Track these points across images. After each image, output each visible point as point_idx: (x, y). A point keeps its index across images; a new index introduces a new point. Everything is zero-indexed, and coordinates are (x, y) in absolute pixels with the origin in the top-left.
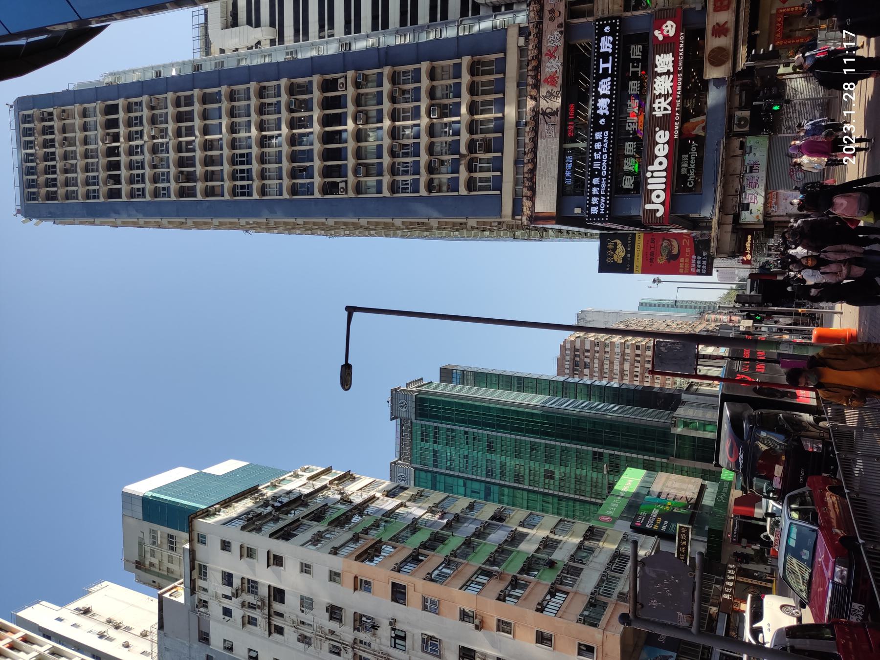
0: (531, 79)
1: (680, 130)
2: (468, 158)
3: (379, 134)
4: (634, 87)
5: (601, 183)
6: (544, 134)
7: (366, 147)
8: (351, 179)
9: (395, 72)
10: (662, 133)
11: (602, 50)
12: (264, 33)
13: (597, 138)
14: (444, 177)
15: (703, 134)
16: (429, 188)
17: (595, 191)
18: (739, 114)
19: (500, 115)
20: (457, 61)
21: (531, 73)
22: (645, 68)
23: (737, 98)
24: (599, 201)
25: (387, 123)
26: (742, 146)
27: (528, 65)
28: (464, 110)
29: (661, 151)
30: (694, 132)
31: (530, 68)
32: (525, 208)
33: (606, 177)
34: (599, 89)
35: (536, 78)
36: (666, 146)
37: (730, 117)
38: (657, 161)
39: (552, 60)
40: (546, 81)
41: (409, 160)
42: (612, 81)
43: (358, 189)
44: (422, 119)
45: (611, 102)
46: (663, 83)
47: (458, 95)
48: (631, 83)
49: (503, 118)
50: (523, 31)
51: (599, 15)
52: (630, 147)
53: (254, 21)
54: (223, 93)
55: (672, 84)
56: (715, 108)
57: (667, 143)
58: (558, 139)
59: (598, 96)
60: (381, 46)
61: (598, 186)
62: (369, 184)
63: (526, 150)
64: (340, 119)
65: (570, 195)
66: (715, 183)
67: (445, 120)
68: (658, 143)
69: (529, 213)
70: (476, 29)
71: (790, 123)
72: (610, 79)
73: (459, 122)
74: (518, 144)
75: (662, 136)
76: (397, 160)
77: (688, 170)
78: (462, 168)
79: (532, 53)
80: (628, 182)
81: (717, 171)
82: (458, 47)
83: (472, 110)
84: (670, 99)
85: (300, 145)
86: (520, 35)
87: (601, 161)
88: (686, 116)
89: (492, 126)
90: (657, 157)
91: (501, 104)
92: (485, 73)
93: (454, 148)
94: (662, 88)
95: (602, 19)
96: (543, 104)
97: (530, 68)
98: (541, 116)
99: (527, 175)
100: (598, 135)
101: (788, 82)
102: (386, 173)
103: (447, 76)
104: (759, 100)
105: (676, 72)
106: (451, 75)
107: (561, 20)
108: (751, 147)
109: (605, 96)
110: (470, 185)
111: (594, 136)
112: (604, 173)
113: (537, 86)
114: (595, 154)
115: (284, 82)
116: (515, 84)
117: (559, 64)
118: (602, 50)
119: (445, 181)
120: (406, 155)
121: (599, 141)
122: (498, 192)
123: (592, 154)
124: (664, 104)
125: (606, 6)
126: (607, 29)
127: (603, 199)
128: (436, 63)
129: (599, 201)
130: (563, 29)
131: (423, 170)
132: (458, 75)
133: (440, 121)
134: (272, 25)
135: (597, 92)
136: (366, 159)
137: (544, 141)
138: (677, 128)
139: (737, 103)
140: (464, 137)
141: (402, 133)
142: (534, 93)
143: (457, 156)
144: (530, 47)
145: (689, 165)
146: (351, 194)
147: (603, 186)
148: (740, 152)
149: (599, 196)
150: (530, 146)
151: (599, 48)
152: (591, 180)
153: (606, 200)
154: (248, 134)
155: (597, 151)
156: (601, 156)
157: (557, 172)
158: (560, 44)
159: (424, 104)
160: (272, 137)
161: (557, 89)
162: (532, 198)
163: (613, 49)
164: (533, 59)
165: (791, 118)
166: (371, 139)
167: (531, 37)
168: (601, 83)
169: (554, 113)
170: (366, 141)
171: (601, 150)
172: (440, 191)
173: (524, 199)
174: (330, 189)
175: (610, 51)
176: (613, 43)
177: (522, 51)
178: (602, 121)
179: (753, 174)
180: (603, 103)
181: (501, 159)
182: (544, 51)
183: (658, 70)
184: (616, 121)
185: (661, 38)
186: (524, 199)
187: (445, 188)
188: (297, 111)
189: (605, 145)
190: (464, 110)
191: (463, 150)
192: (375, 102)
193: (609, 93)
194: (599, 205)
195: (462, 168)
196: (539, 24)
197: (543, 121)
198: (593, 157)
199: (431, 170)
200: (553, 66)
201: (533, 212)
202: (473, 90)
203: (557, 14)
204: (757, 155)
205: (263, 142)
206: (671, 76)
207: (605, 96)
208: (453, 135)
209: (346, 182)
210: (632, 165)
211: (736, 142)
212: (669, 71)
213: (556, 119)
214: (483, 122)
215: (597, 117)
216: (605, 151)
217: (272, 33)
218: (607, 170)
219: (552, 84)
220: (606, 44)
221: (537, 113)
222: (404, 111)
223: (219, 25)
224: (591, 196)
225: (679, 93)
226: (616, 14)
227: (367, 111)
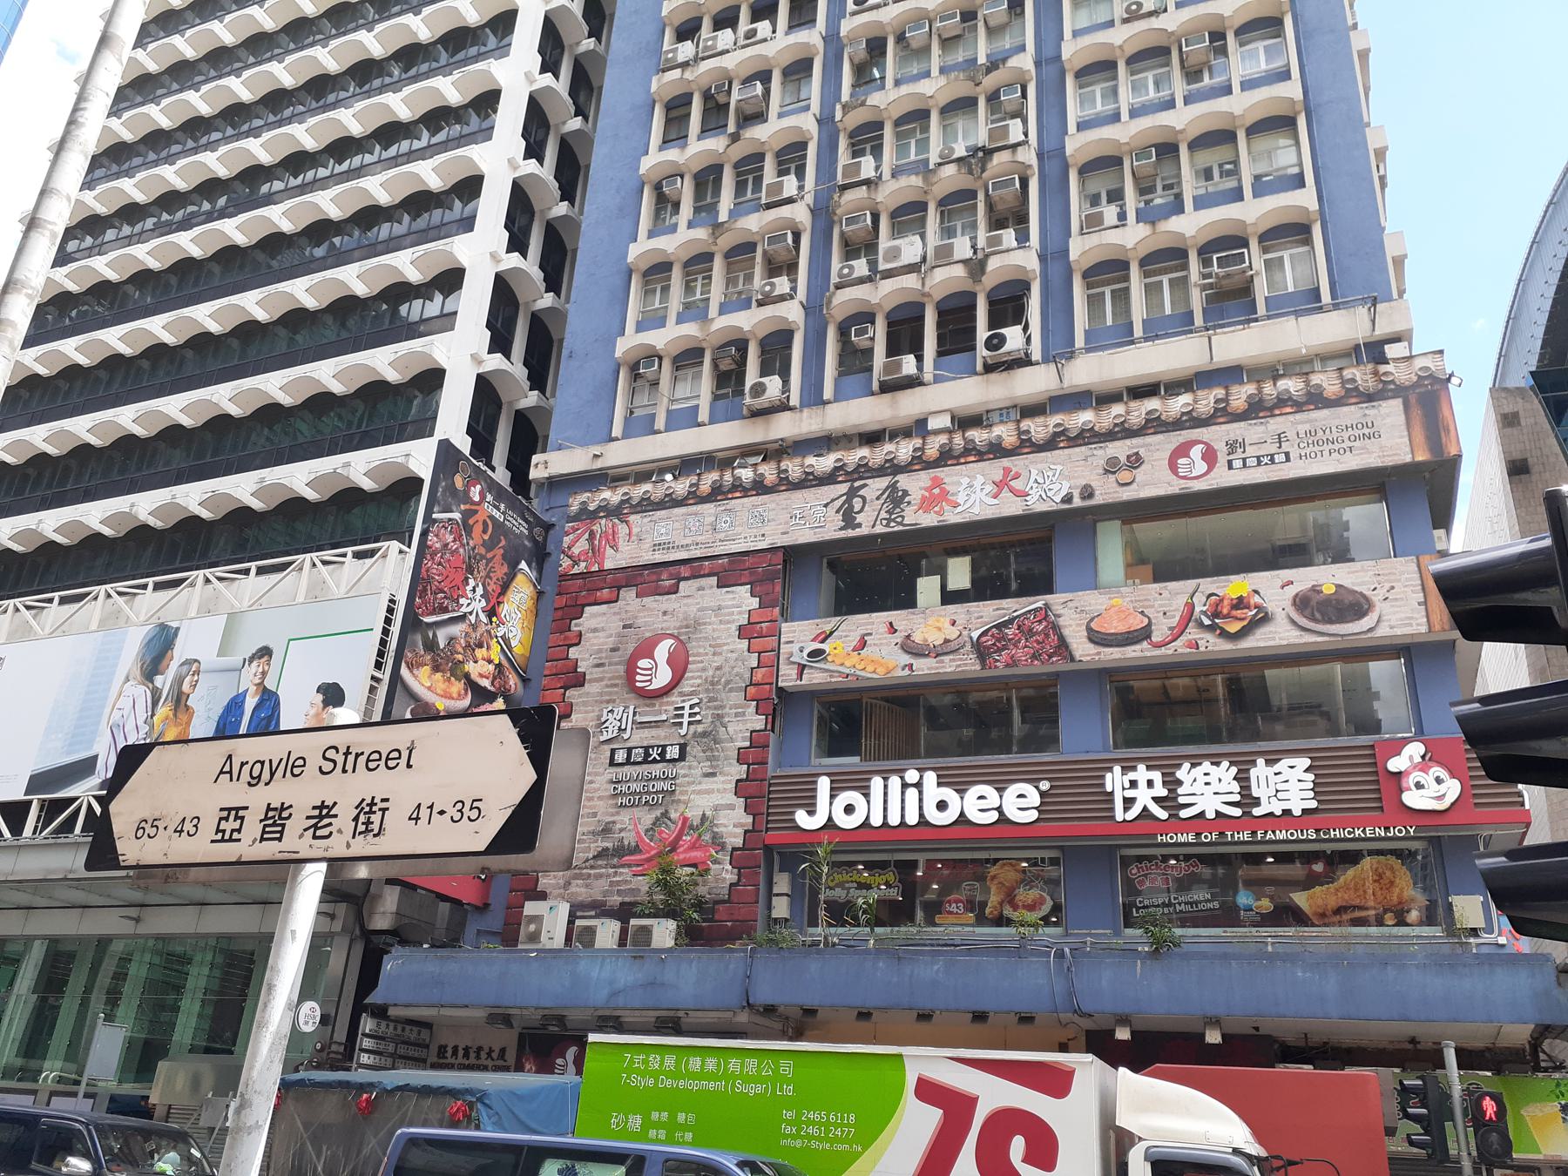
55: (1210, 815)
84: (1162, 814)
94: (1199, 787)
183: (1260, 771)
206: (1237, 812)
212: (1257, 802)
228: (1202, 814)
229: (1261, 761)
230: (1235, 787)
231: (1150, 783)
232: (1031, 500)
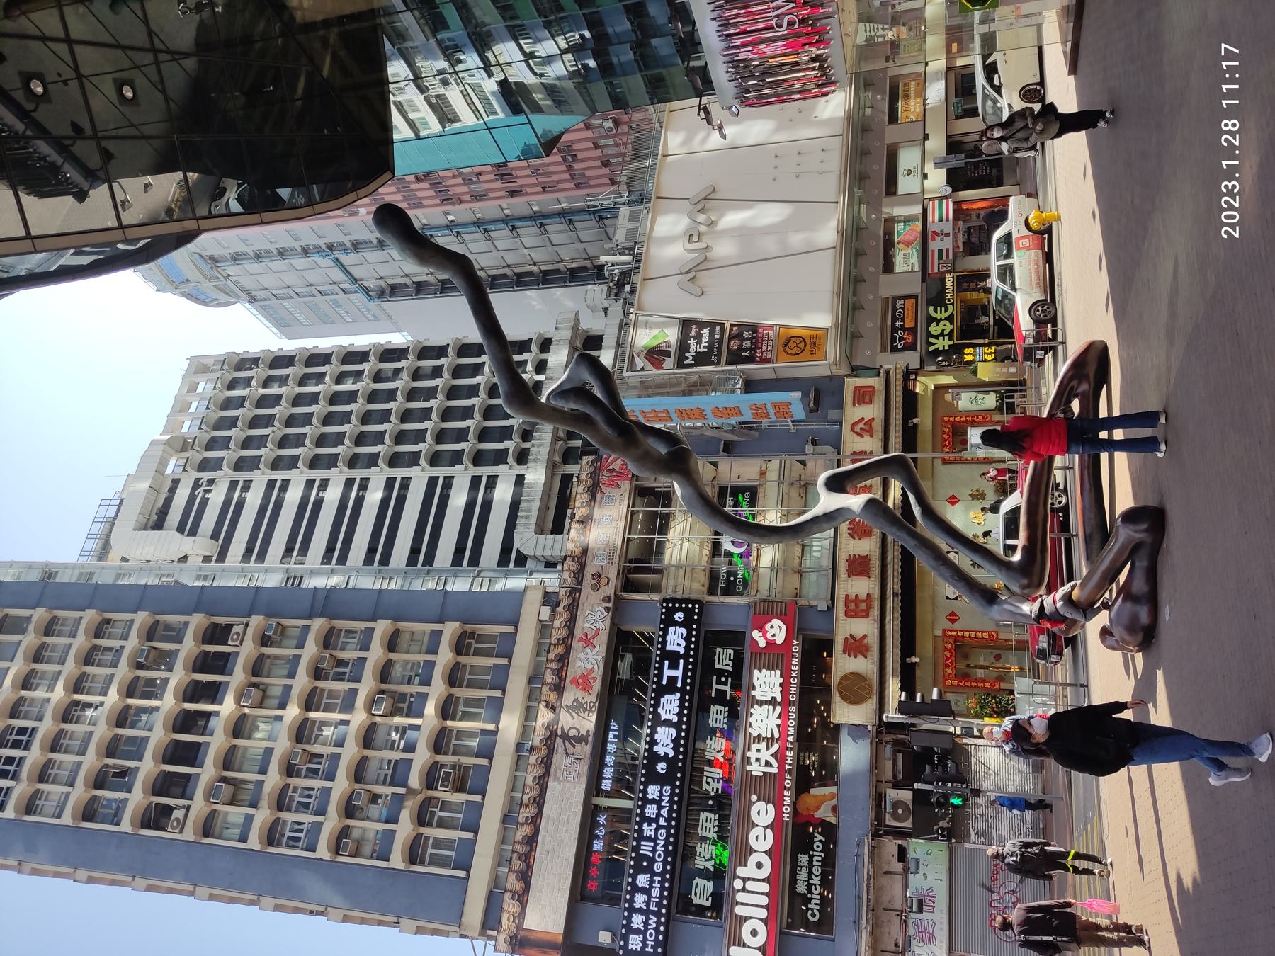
0: (552, 676)
1: (794, 805)
2: (421, 797)
3: (274, 734)
4: (718, 716)
5: (651, 887)
6: (560, 774)
7: (246, 748)
8: (199, 805)
9: (332, 628)
10: (761, 805)
11: (668, 648)
12: (199, 546)
13: (650, 796)
14: (367, 828)
15: (833, 820)
16: (337, 848)
17: (640, 900)
18: (893, 794)
19: (491, 727)
20: (370, 624)
21: (553, 665)
22: (737, 686)
23: (889, 764)
24: (646, 924)
25: (293, 712)
26: (902, 854)
27: (548, 652)
28: (430, 709)
29: (761, 840)
30: (818, 815)
31: (551, 656)
32: (505, 917)
33: (662, 874)
34: (660, 710)
35: (560, 673)
36: (769, 832)
37: (879, 798)
38: (752, 860)
39: (588, 650)
40: (574, 681)
41: (316, 784)
42: (682, 700)
43: (207, 829)
44: (355, 712)
45: (678, 736)
46: (764, 717)
47: (427, 682)
48: (714, 708)
49: (495, 733)
50: (549, 599)
51: (669, 593)
52: (708, 822)
53: (189, 527)
54: (34, 619)
55: (779, 722)
56: (853, 776)
57: (771, 826)
58: (583, 786)
59: (658, 722)
60: (350, 587)
61: (646, 891)
62: (231, 819)
63: (526, 798)
64: (212, 692)
65: (594, 900)
66: (857, 922)
67: (398, 720)
68: (754, 825)
69: (513, 927)
70: (499, 586)
71: (984, 826)
72: (678, 695)
73: (417, 728)
74: (514, 784)
75: (762, 813)
76: (294, 781)
77: (810, 886)
78: (406, 816)
79: (558, 633)
80: (702, 891)
81: (860, 898)
82: (444, 607)
83: (446, 710)
84: (776, 747)
85: (132, 727)
86: (545, 603)
87: (655, 841)
88: (804, 782)
89: (474, 743)
90: (752, 851)
91: (497, 707)
92: (478, 653)
93: (398, 774)
94: (763, 726)
95: (674, 600)
96: (567, 721)
97: (551, 656)
98: (559, 741)
99: (520, 848)
100: (653, 791)
101: (972, 750)
102: (264, 803)
103: (417, 648)
104: (927, 778)
105: (786, 703)
106: (424, 648)
107: (609, 590)
108: (917, 861)
109: (668, 723)
110: (415, 853)
111: (645, 792)
112: (658, 867)
113: (559, 688)
114: (645, 826)
115: (141, 618)
116: (524, 679)
117: (599, 658)
118: (668, 648)
119: (371, 835)
120: (313, 773)
121: (653, 801)
122: (463, 874)
123: (640, 824)
124: (766, 755)
125: (680, 581)
126: (679, 616)
127: (653, 920)
128: (402, 625)
129: (646, 924)
130: (610, 605)
131: (332, 809)
132: (433, 650)
133: (387, 720)
134: (215, 536)
135: (656, 715)
136: (239, 771)
137: (558, 786)
138: (787, 801)
139: (889, 774)
140: (422, 757)
141: (316, 732)
142: (552, 698)
143: (402, 791)
144: (557, 624)
145: (810, 878)
146: (189, 835)
147: (656, 892)
148: (898, 866)
149: (646, 912)
150: (533, 791)
151: (664, 643)
152: (634, 877)
153: (658, 923)
154: (47, 695)
155: (650, 821)
156: (656, 831)
157: (574, 851)
158: (605, 626)
159: (366, 686)
160: (89, 705)
161: (591, 698)
162: (522, 897)
163: (687, 648)
164: (558, 643)
165: (984, 816)
166: (258, 735)
167: (560, 609)
168: (663, 700)
169: (581, 739)
170: (249, 738)
171: (656, 820)
172: (356, 854)
173: (508, 896)
174: (156, 817)
175: (682, 651)
176: (687, 639)
177: (544, 627)
178: (661, 767)
179: (925, 915)
180: (665, 737)
181: (479, 807)
182: (578, 633)
183: (758, 694)
184: (687, 765)
185: (762, 643)
186: (508, 896)
187: (367, 849)
188: (148, 668)
189: (664, 812)
190: (430, 709)
191: (414, 781)
192: (285, 672)
193: (675, 719)
194: (644, 933)
195: (406, 816)
196: (575, 592)
197: (561, 750)
198: (640, 831)
199: (350, 810)
200: (589, 660)
201: (519, 926)
202: (454, 678)
203: (603, 581)
204: (930, 877)
205: (69, 713)
206: (778, 709)
207: (668, 723)
208: (404, 750)
209: (188, 808)
210: (706, 856)
211: (891, 845)
212: (774, 698)
213: (585, 750)
214: (461, 734)
215: (653, 758)
216: (662, 822)
217: (213, 548)
218: (665, 862)
219: (583, 689)
220: (676, 639)
221: (552, 735)
222: (332, 694)
223: (133, 524)
224: (632, 910)
225: (791, 739)
226: (694, 596)
227: (267, 685)
228: (778, 726)
229: (753, 693)
230: (765, 707)
231: (758, 751)
232: (602, 626)
